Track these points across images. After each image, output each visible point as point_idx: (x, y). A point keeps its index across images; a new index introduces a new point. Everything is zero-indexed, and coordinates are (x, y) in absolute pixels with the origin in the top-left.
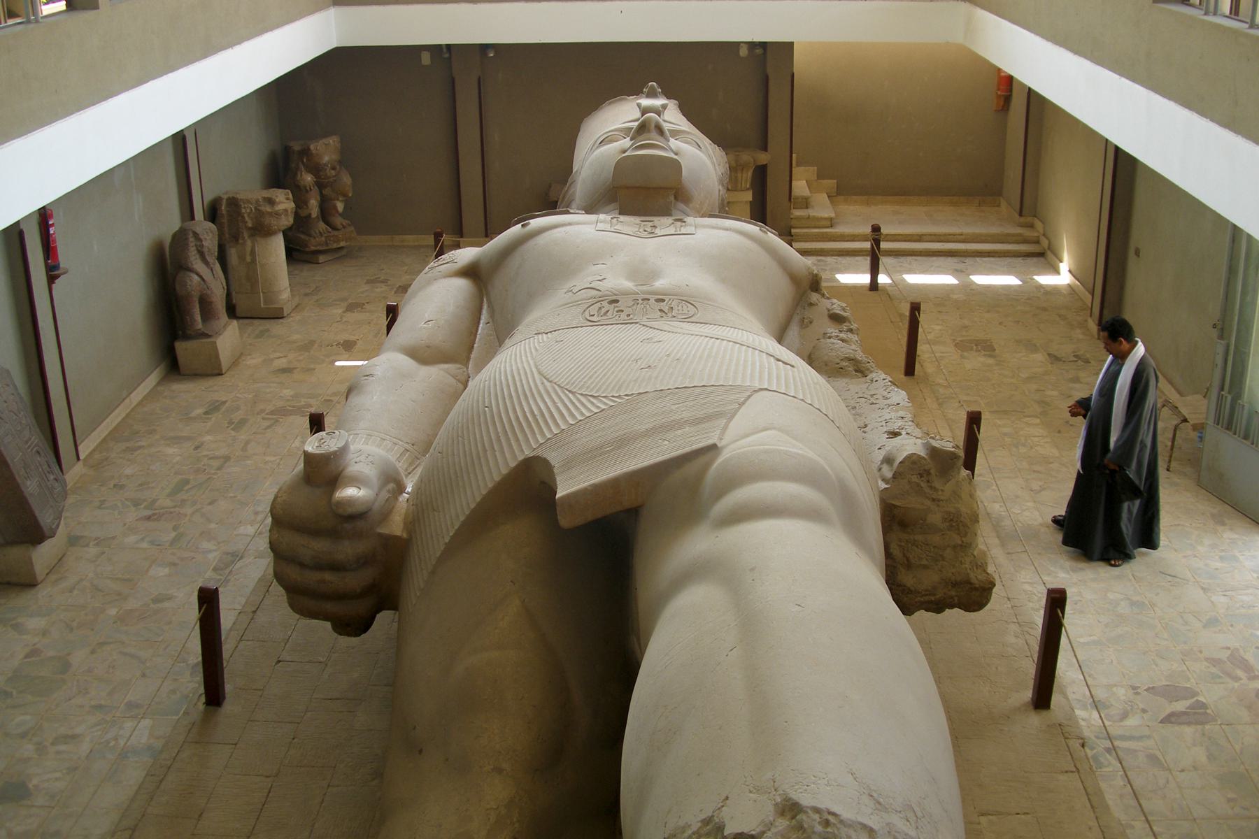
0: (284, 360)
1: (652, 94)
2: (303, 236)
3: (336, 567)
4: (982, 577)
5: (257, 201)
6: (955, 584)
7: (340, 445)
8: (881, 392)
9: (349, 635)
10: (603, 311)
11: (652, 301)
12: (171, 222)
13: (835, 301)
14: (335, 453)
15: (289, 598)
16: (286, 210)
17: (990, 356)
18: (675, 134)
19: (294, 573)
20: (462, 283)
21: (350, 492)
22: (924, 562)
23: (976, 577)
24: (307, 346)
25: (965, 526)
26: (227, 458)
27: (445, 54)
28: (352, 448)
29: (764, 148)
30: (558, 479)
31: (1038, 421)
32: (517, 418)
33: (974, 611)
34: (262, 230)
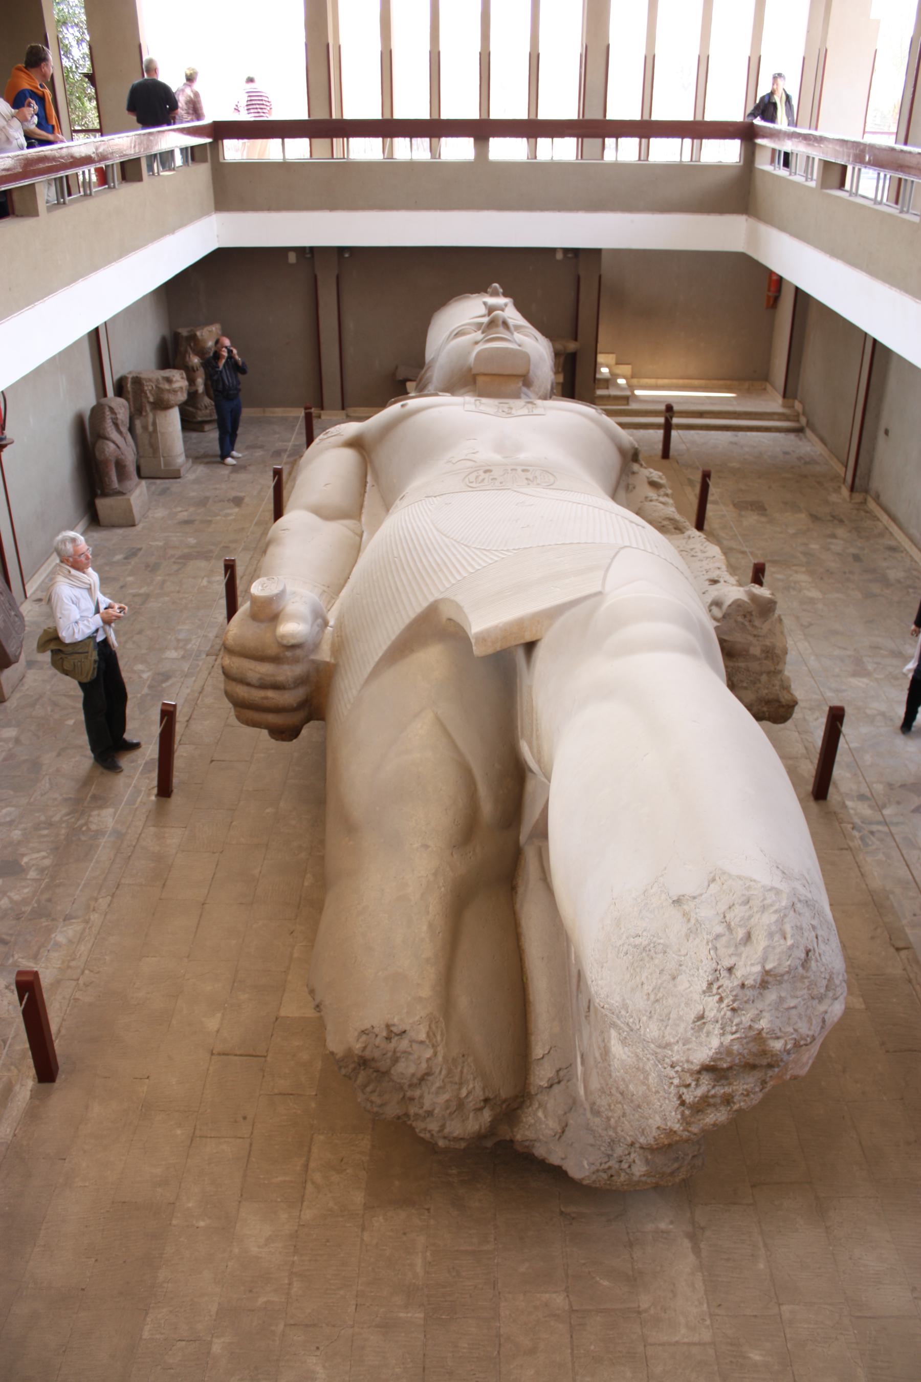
0: (185, 513)
1: (495, 294)
2: (191, 409)
3: (277, 687)
4: (787, 697)
5: (157, 380)
6: (768, 702)
7: (281, 588)
8: (698, 547)
9: (283, 740)
10: (481, 478)
11: (519, 471)
12: (87, 400)
13: (652, 470)
14: (277, 595)
15: (235, 711)
16: (181, 388)
17: (763, 515)
18: (518, 328)
19: (242, 691)
20: (349, 455)
21: (293, 627)
22: (745, 685)
23: (784, 698)
24: (203, 502)
25: (778, 656)
26: (147, 597)
27: (309, 254)
28: (289, 589)
29: (576, 339)
30: (471, 617)
31: (804, 569)
32: (424, 566)
33: (781, 723)
34: (161, 405)
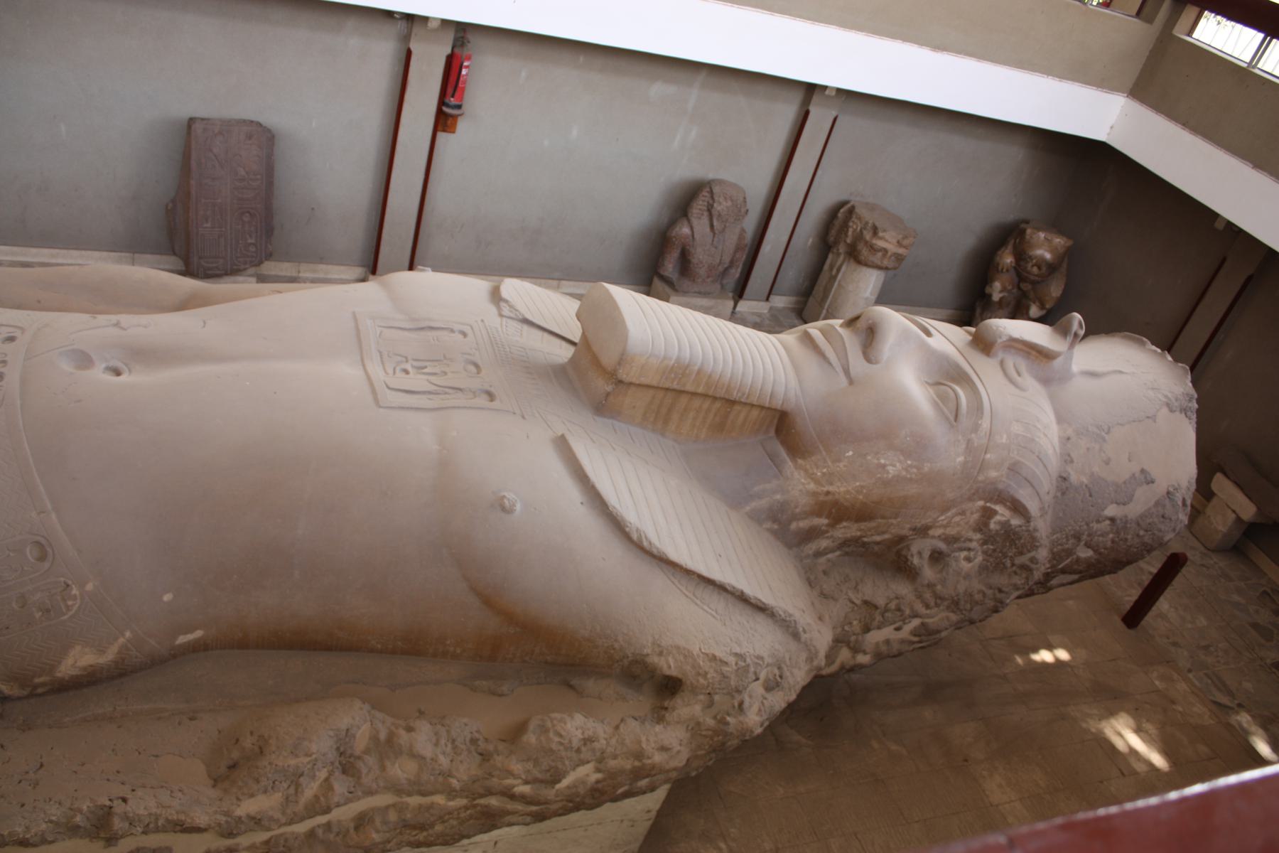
1: (1064, 332)
16: (885, 251)
34: (853, 255)
